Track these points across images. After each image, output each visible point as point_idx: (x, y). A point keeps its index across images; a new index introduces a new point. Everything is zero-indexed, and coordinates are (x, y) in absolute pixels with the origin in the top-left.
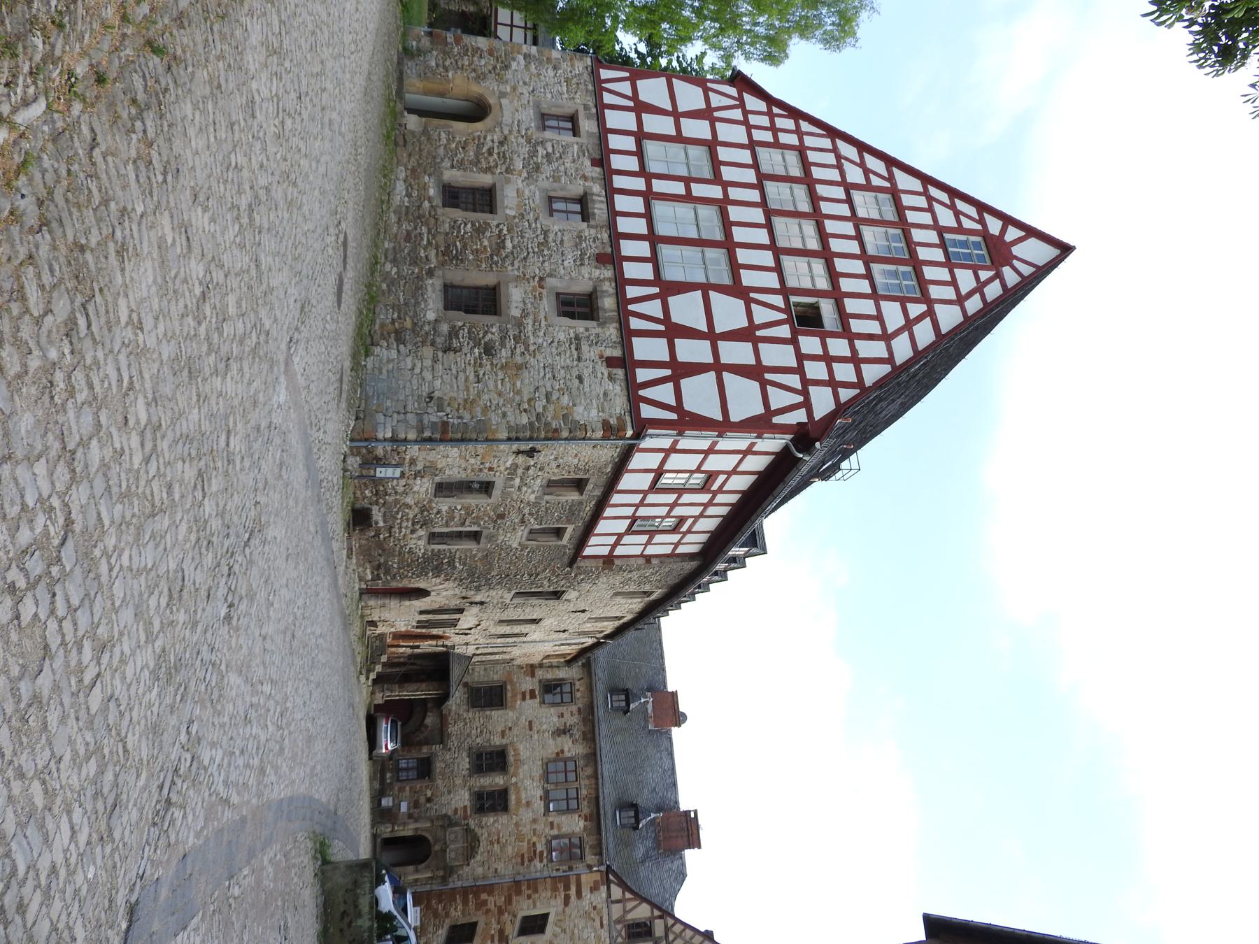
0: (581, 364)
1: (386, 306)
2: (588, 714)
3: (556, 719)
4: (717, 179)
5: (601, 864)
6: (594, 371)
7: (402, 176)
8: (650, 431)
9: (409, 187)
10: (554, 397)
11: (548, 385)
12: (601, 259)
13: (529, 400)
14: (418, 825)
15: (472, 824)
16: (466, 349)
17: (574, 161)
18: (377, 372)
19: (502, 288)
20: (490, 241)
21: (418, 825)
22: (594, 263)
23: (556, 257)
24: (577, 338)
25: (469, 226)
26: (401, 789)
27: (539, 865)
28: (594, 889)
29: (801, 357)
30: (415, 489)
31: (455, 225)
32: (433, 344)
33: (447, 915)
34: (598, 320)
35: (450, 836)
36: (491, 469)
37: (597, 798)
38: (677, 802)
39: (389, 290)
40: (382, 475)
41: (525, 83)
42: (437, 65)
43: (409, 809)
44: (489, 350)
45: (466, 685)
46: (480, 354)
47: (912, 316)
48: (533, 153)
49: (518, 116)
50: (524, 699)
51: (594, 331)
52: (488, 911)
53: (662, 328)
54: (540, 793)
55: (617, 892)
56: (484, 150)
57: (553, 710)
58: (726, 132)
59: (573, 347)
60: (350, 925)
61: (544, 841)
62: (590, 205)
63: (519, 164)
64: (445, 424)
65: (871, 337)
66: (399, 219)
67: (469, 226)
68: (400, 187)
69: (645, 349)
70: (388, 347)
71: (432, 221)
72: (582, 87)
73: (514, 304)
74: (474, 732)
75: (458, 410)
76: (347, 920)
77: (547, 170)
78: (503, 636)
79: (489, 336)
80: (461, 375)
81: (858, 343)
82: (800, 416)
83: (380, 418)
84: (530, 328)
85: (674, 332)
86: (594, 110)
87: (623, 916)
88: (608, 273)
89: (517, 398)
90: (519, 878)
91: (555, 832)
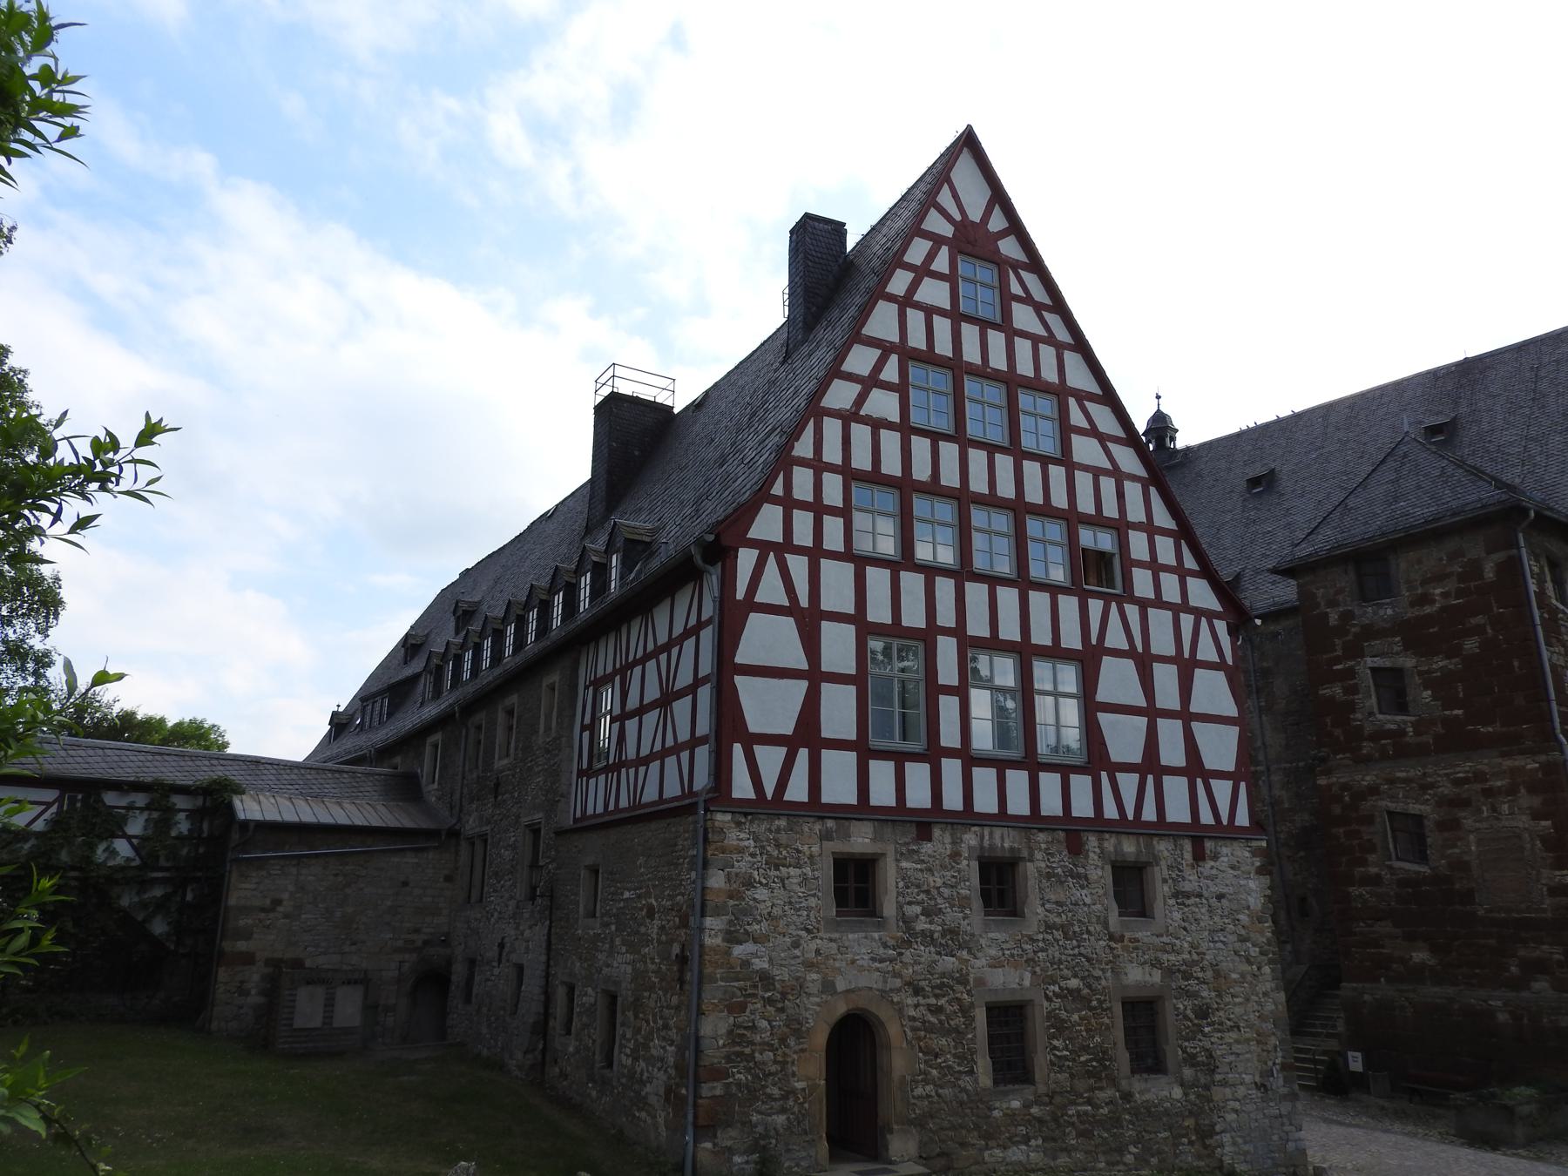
1: (1176, 1156)
6: (1212, 878)
9: (1013, 1141)
10: (1243, 932)
12: (1075, 847)
13: (1250, 963)
17: (930, 870)
18: (1248, 1158)
23: (1082, 912)
24: (1176, 895)
25: (1055, 1042)
31: (1057, 1064)
32: (1207, 1088)
34: (1149, 864)
41: (796, 945)
42: (783, 1110)
44: (1203, 1013)
46: (1209, 1025)
48: (928, 937)
49: (864, 961)
56: (933, 1020)
62: (999, 854)
63: (949, 963)
67: (1055, 1042)
68: (1016, 1154)
72: (783, 838)
73: (1147, 978)
77: (952, 916)
79: (1188, 1012)
84: (1172, 958)
85: (1150, 765)
86: (830, 824)
88: (1092, 842)
89: (1249, 978)
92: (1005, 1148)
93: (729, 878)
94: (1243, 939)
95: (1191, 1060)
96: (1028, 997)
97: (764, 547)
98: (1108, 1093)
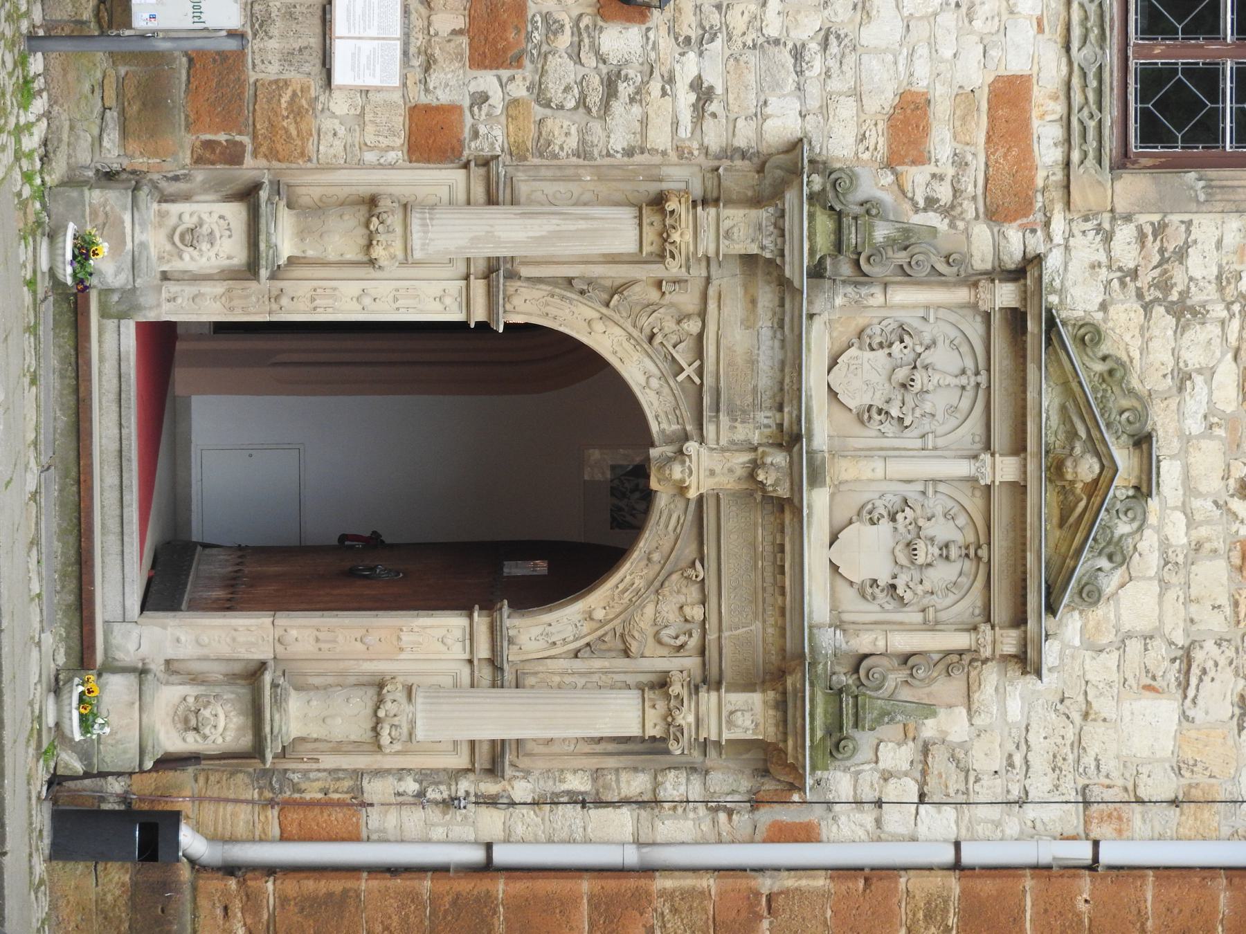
14: (508, 232)
35: (843, 371)
43: (420, 58)
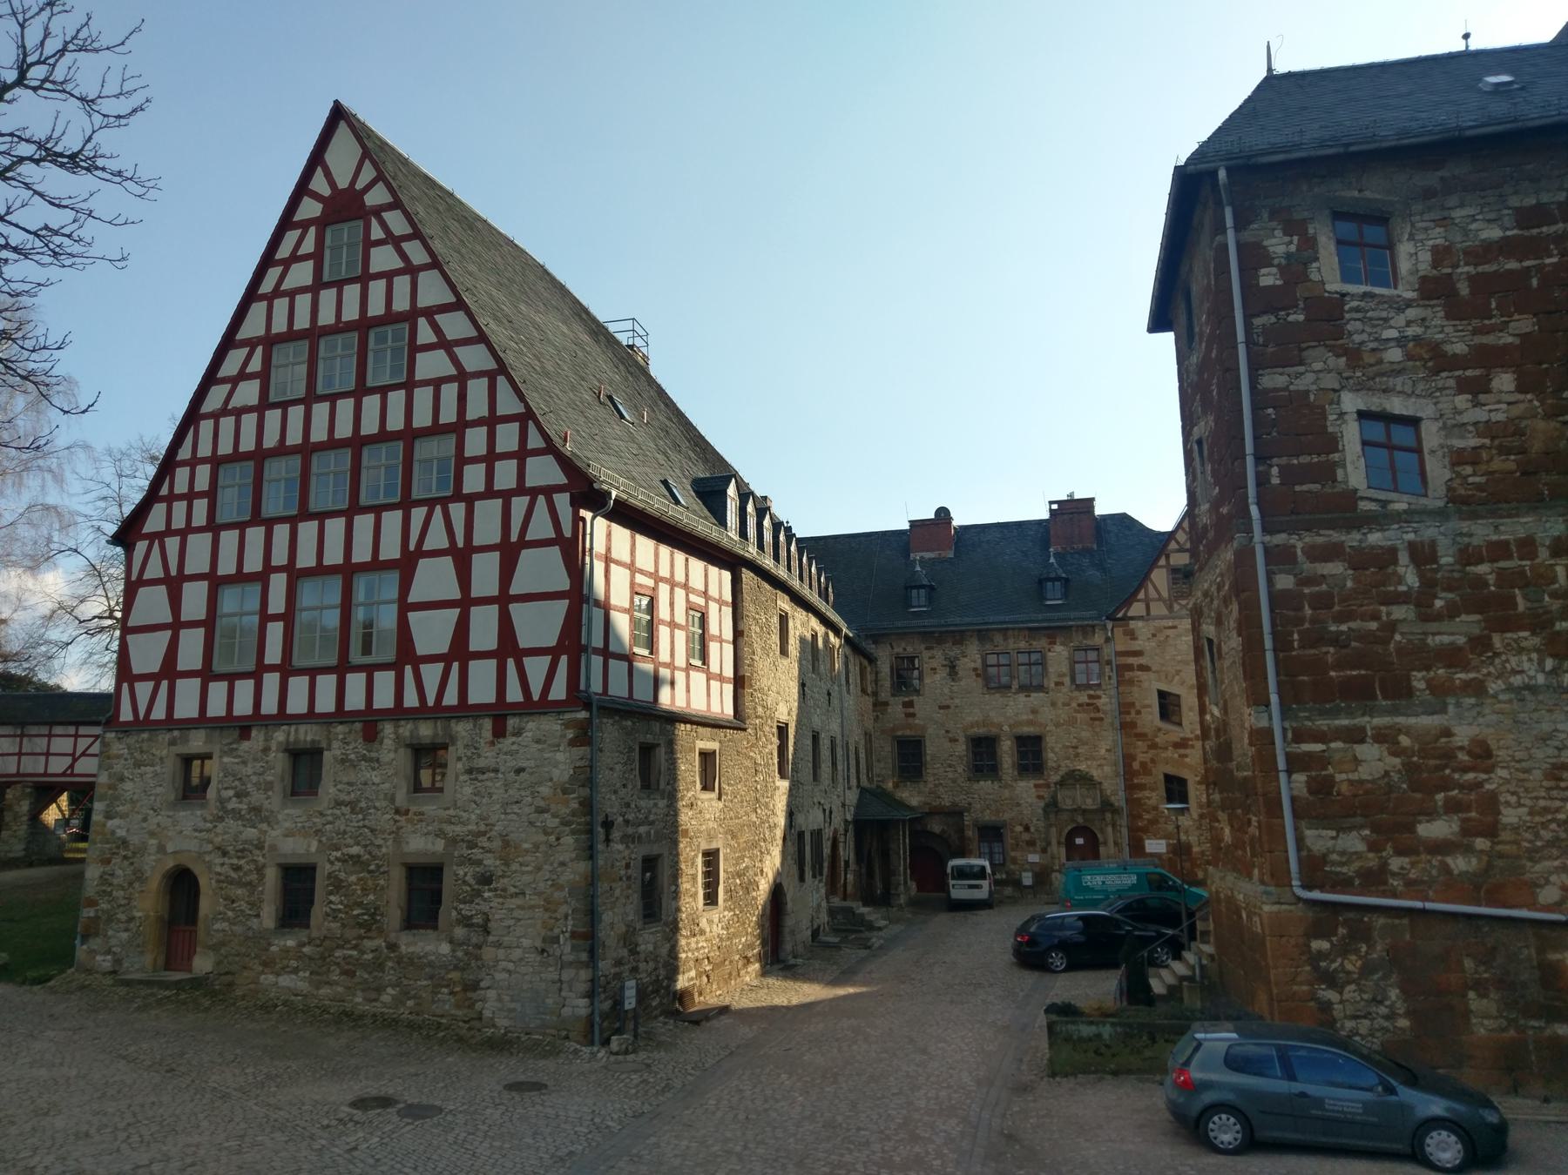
0: (502, 769)
1: (433, 1002)
2: (933, 638)
3: (938, 677)
4: (262, 578)
5: (1104, 628)
7: (271, 978)
8: (582, 687)
9: (284, 970)
10: (542, 804)
11: (527, 810)
12: (371, 734)
13: (546, 833)
14: (1054, 841)
15: (1055, 778)
16: (485, 907)
17: (244, 763)
19: (410, 860)
20: (352, 873)
21: (1054, 841)
22: (376, 745)
24: (470, 771)
25: (332, 898)
26: (1014, 861)
27: (1104, 700)
28: (1132, 635)
29: (489, 493)
30: (650, 948)
31: (333, 915)
32: (480, 947)
33: (1156, 808)
36: (628, 866)
37: (1030, 629)
38: (1040, 522)
39: (414, 997)
40: (633, 1001)
41: (145, 820)
42: (126, 930)
43: (1035, 852)
44: (486, 879)
45: (896, 786)
47: (434, 339)
48: (237, 815)
50: (913, 715)
51: (461, 751)
52: (1153, 761)
53: (456, 665)
54: (1021, 697)
55: (1137, 609)
56: (233, 875)
57: (927, 681)
58: (198, 560)
59: (481, 777)
60: (1107, 1046)
61: (1076, 694)
63: (251, 833)
64: (574, 935)
65: (462, 398)
66: (327, 983)
67: (332, 898)
68: (285, 981)
69: (482, 689)
70: (484, 1000)
71: (327, 943)
72: (145, 746)
73: (430, 846)
74: (950, 775)
75: (557, 919)
76: (1103, 1050)
77: (257, 797)
78: (834, 764)
80: (516, 914)
81: (470, 416)
82: (562, 501)
83: (566, 1011)
84: (458, 829)
85: (459, 652)
86: (176, 733)
87: (1164, 601)
88: (388, 729)
90: (1117, 724)
91: (1067, 680)
92: (278, 975)
93: (110, 777)
94: (540, 811)
95: (466, 921)
96: (312, 860)
97: (152, 537)
98: (380, 942)
